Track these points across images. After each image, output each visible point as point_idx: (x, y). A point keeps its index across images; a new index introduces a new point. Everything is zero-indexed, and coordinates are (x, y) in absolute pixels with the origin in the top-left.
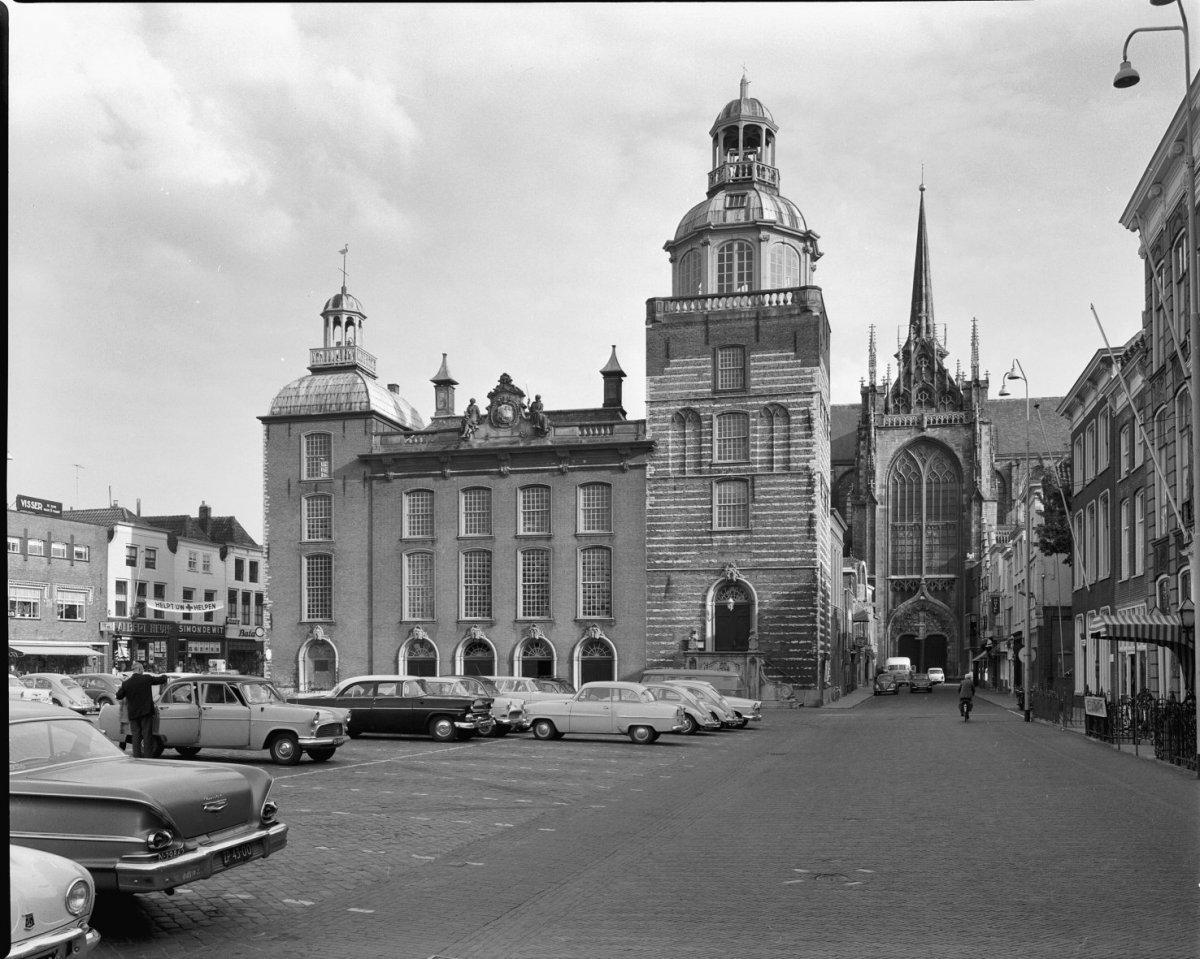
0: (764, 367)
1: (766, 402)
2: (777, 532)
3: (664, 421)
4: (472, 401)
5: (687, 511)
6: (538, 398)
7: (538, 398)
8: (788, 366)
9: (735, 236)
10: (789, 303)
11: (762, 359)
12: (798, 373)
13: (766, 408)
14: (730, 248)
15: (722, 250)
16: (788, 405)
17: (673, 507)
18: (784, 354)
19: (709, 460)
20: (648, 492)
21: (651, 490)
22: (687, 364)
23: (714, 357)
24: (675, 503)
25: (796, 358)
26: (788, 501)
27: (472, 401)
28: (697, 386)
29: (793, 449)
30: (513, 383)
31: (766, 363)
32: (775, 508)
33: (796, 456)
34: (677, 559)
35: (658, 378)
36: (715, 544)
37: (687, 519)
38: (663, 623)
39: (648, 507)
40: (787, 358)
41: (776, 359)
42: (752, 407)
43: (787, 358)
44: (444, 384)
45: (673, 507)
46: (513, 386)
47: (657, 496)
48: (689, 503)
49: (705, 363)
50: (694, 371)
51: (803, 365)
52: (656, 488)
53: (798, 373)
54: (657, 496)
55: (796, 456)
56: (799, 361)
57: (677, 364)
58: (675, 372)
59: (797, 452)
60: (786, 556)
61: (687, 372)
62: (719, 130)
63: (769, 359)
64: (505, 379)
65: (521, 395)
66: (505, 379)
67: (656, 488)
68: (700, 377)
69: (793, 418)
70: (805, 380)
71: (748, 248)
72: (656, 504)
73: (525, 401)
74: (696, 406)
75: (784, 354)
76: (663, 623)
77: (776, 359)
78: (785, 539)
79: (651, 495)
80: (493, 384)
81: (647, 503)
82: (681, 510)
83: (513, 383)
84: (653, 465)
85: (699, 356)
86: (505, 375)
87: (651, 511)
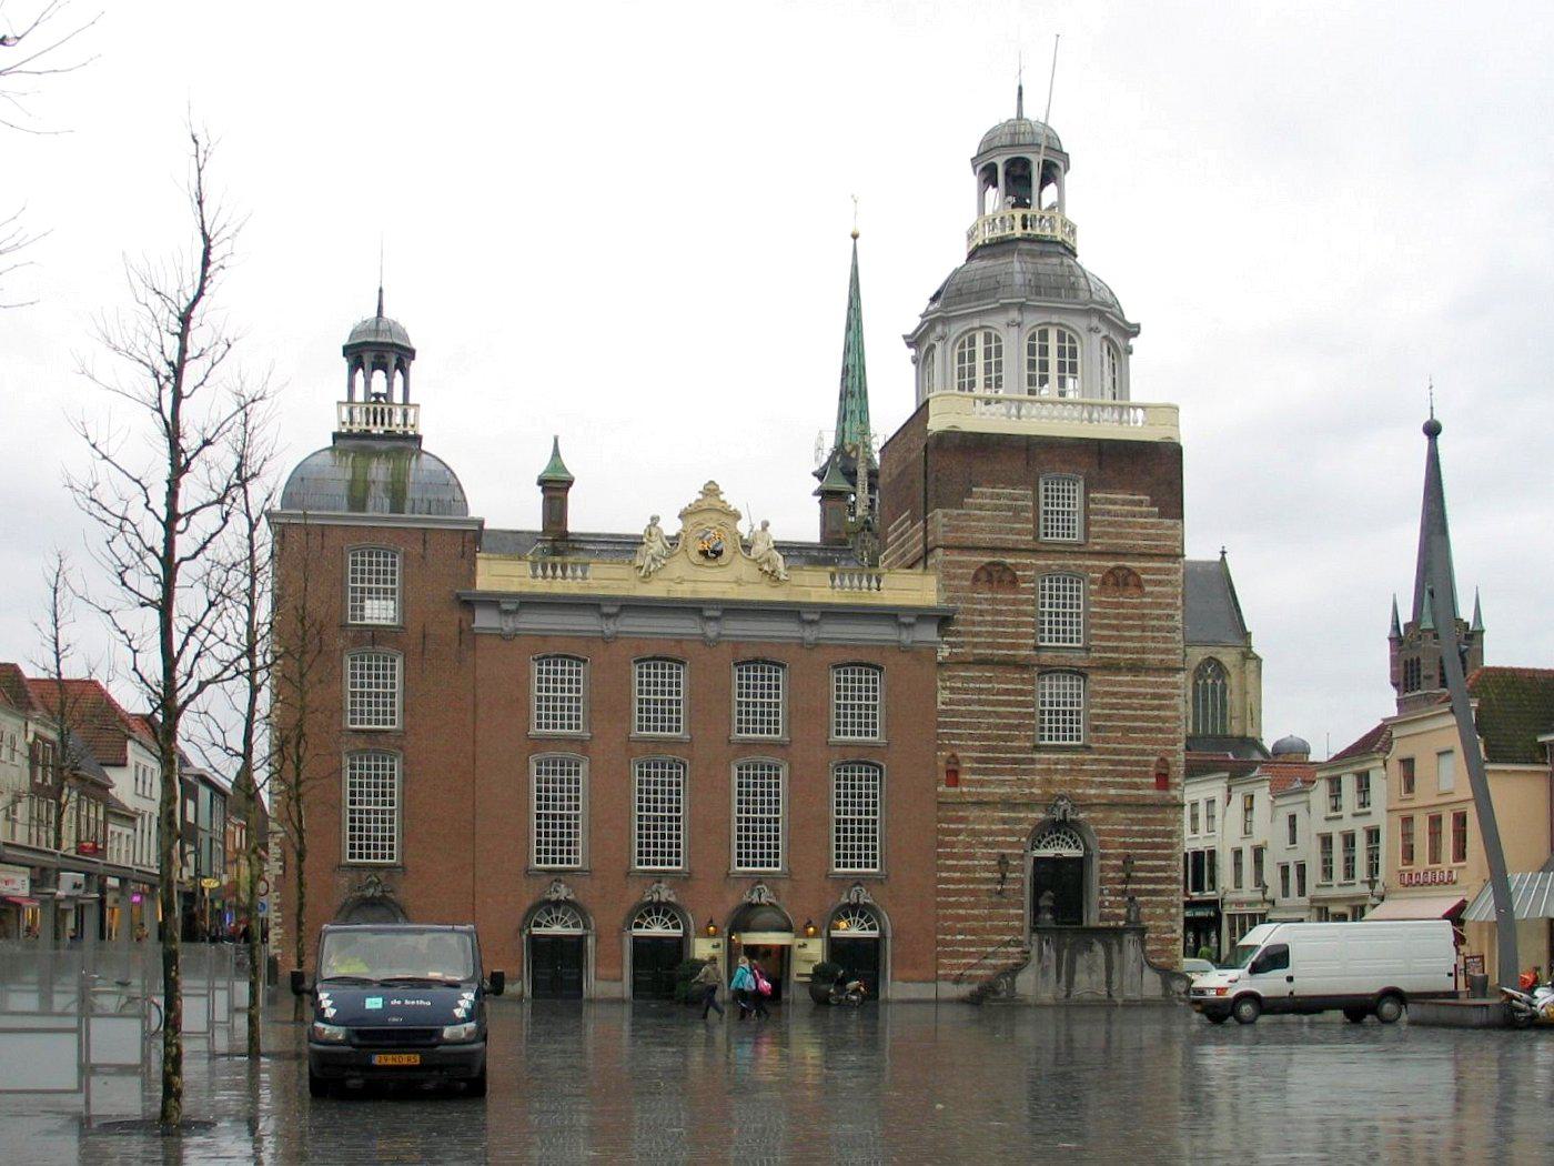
0: (1109, 513)
1: (1112, 564)
2: (1130, 752)
3: (962, 577)
5: (998, 715)
8: (1142, 515)
9: (1055, 319)
10: (1140, 424)
12: (1153, 526)
13: (1112, 572)
14: (1044, 335)
15: (1032, 338)
16: (1145, 571)
17: (976, 708)
18: (1136, 497)
20: (939, 684)
21: (943, 680)
22: (999, 497)
23: (1036, 490)
24: (979, 702)
25: (1152, 505)
26: (1142, 707)
28: (1012, 530)
30: (722, 497)
31: (1111, 507)
32: (1125, 718)
33: (1153, 645)
34: (982, 786)
35: (956, 512)
36: (1039, 767)
37: (997, 726)
38: (960, 881)
40: (1140, 503)
41: (1125, 503)
42: (1093, 569)
43: (1140, 503)
44: (555, 487)
45: (976, 708)
46: (724, 502)
47: (952, 690)
49: (1025, 497)
50: (1009, 508)
51: (1162, 515)
52: (951, 678)
53: (1153, 526)
55: (1153, 645)
57: (983, 495)
60: (1136, 786)
61: (996, 508)
62: (1000, 162)
63: (1114, 502)
64: (711, 490)
65: (737, 516)
66: (711, 490)
70: (1168, 537)
71: (1072, 340)
72: (951, 702)
74: (1009, 561)
75: (1136, 497)
76: (960, 881)
77: (1125, 503)
78: (1137, 763)
80: (692, 495)
81: (940, 699)
82: (989, 714)
83: (722, 497)
84: (948, 643)
85: (1013, 485)
86: (711, 482)
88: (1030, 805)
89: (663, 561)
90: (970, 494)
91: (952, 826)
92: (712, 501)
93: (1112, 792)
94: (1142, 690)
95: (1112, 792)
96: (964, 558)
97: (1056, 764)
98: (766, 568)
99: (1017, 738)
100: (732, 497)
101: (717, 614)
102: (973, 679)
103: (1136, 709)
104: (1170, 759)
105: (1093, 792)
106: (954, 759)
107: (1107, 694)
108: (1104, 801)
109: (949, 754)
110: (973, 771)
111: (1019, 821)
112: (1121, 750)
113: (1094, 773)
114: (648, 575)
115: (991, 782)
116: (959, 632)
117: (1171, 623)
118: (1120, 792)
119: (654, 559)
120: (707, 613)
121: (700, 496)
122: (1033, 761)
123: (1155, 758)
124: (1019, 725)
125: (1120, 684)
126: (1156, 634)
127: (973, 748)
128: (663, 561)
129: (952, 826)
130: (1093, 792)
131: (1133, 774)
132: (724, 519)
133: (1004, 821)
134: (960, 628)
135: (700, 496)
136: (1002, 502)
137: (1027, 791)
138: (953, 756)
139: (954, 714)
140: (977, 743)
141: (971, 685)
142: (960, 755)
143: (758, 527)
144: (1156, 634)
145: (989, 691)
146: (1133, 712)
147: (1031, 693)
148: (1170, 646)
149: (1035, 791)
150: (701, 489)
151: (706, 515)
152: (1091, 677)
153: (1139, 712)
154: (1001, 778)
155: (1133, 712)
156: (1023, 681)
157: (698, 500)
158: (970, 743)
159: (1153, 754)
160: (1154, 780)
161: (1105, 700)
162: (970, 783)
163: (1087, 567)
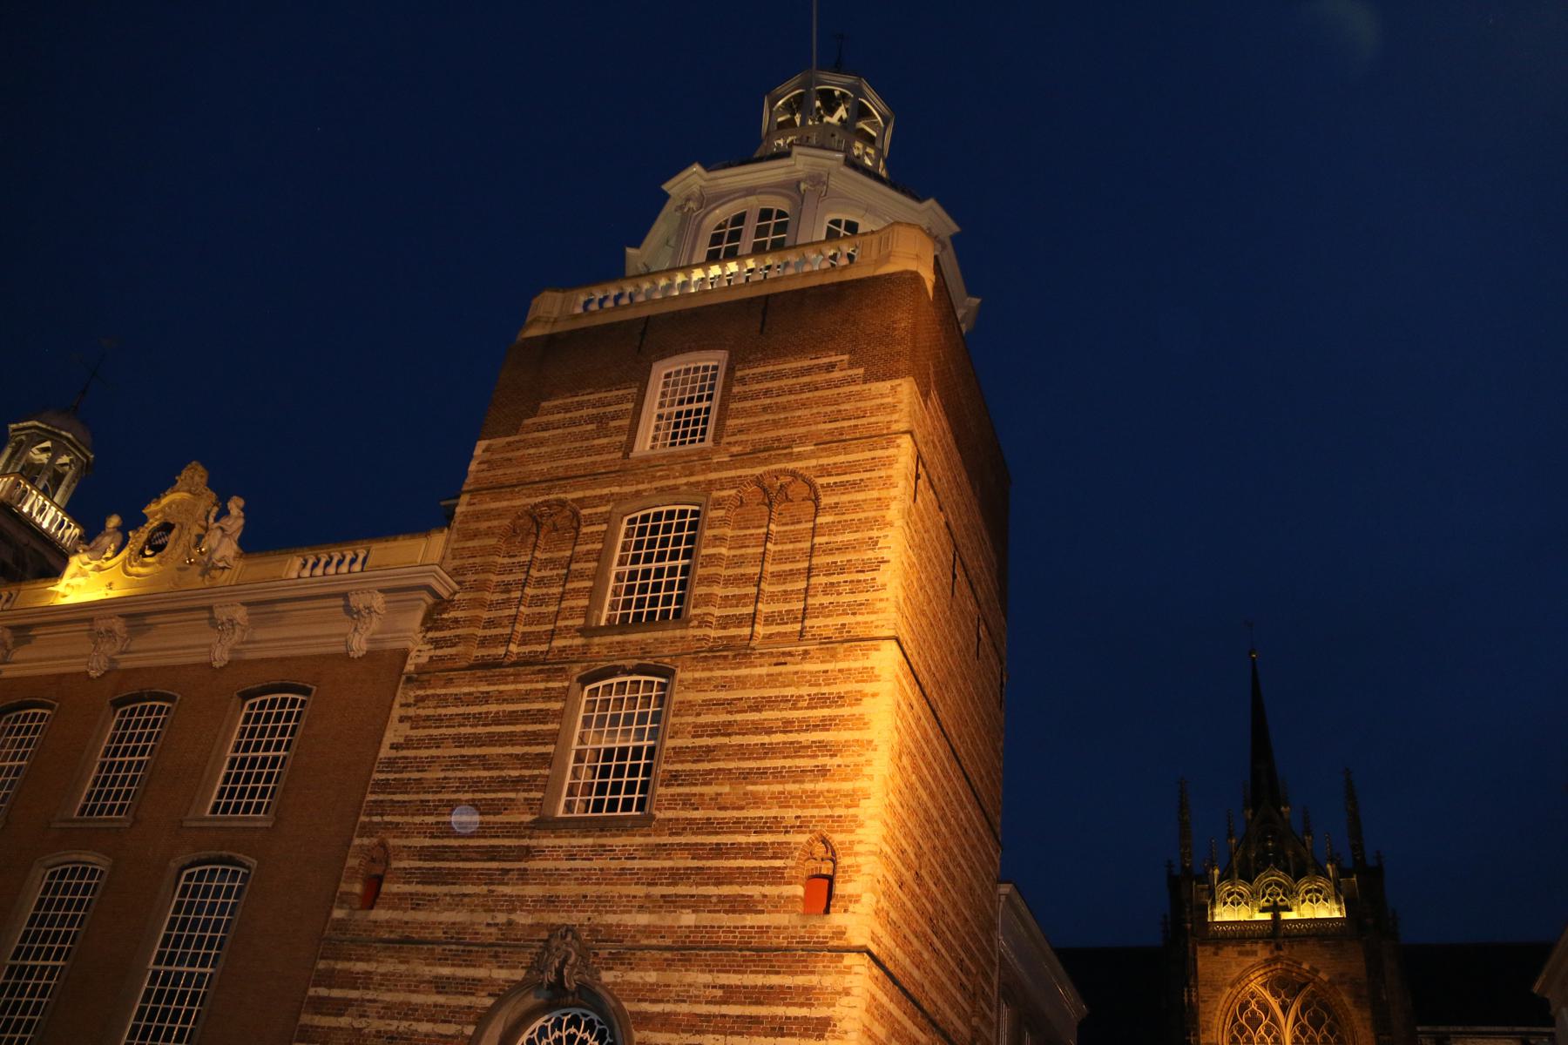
11: (764, 377)
16: (825, 471)
19: (581, 621)
20: (397, 711)
22: (580, 406)
24: (461, 741)
25: (852, 365)
29: (819, 580)
33: (826, 600)
39: (385, 752)
47: (415, 722)
48: (493, 740)
52: (419, 700)
54: (415, 722)
55: (826, 600)
56: (861, 371)
58: (546, 427)
59: (829, 589)
67: (419, 700)
68: (603, 431)
69: (825, 501)
72: (408, 743)
79: (402, 720)
81: (389, 737)
82: (466, 761)
87: (391, 763)
88: (502, 947)
90: (534, 412)
91: (336, 993)
93: (688, 919)
94: (789, 692)
95: (688, 919)
96: (494, 505)
97: (571, 857)
99: (507, 805)
102: (459, 700)
103: (769, 732)
104: (836, 838)
105: (643, 919)
106: (383, 854)
107: (710, 705)
108: (668, 942)
109: (375, 840)
110: (408, 875)
111: (470, 986)
112: (722, 822)
113: (655, 877)
115: (434, 899)
116: (456, 621)
117: (870, 554)
118: (706, 919)
122: (528, 853)
123: (803, 838)
124: (518, 781)
125: (742, 682)
126: (834, 579)
127: (423, 830)
129: (336, 993)
130: (643, 919)
131: (745, 876)
133: (440, 985)
134: (459, 614)
136: (584, 412)
137: (502, 918)
138: (383, 845)
139: (408, 764)
140: (430, 819)
141: (452, 710)
142: (392, 842)
144: (834, 579)
145: (479, 719)
146: (766, 739)
147: (558, 715)
148: (861, 597)
149: (523, 919)
152: (680, 675)
153: (778, 738)
154: (456, 889)
155: (766, 739)
156: (548, 695)
158: (418, 819)
159: (800, 829)
160: (800, 890)
161: (704, 719)
162: (400, 901)
163: (710, 482)
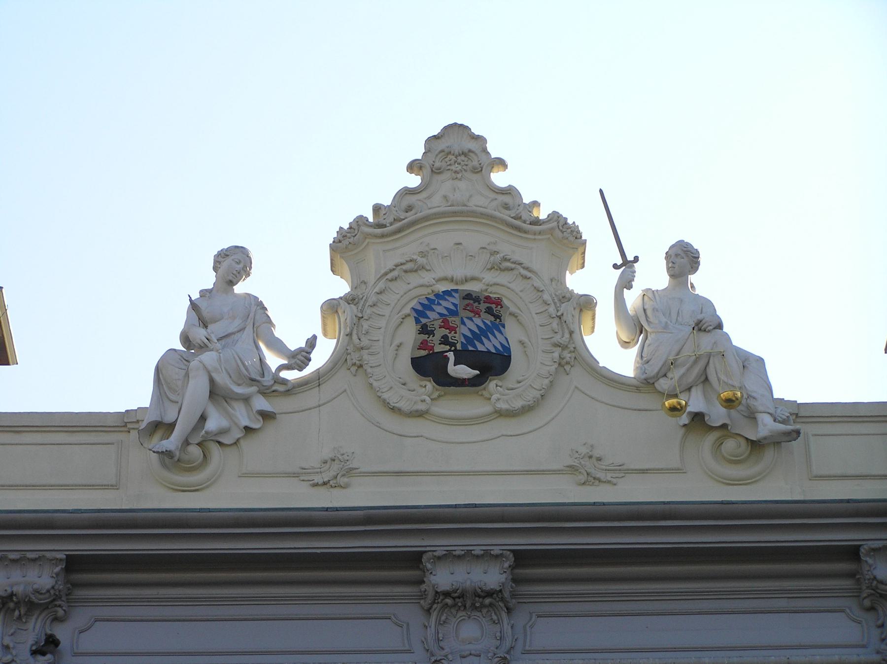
4: (233, 263)
6: (683, 260)
7: (683, 260)
27: (233, 263)
30: (499, 179)
46: (510, 192)
64: (456, 154)
65: (564, 238)
73: (591, 278)
89: (261, 403)
92: (453, 190)
98: (696, 402)
100: (537, 173)
101: (492, 577)
114: (204, 441)
119: (215, 393)
120: (443, 578)
121: (414, 181)
128: (261, 403)
132: (510, 247)
135: (414, 181)
143: (653, 275)
150: (418, 153)
151: (441, 239)
157: (406, 192)
